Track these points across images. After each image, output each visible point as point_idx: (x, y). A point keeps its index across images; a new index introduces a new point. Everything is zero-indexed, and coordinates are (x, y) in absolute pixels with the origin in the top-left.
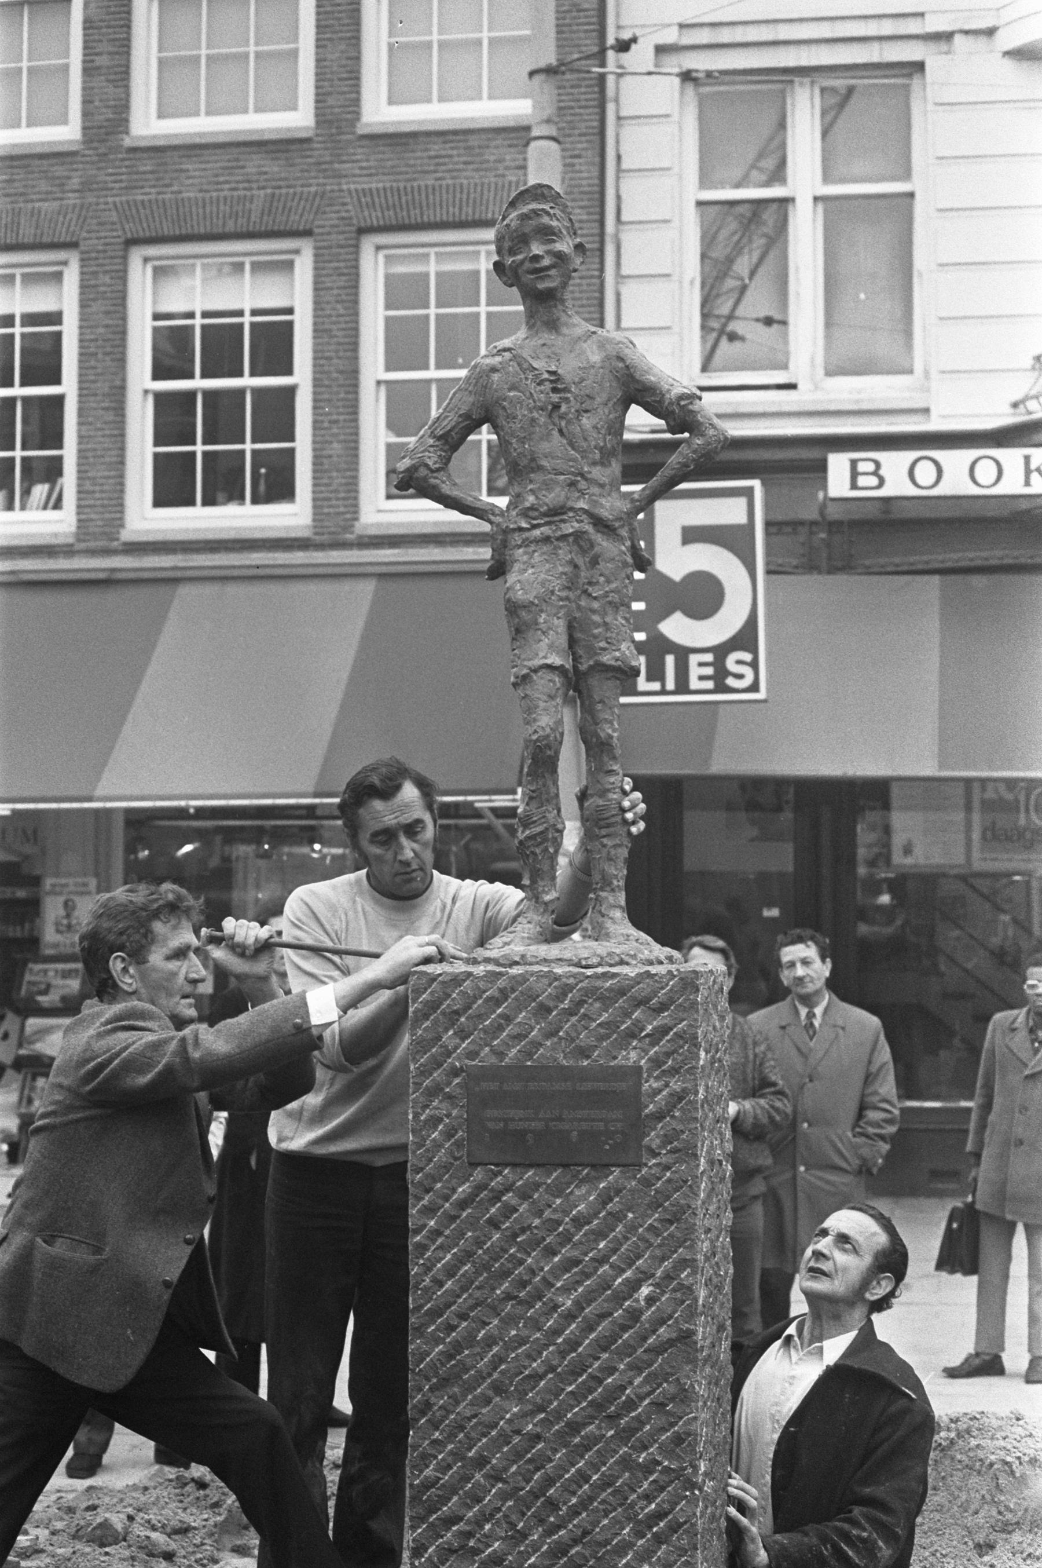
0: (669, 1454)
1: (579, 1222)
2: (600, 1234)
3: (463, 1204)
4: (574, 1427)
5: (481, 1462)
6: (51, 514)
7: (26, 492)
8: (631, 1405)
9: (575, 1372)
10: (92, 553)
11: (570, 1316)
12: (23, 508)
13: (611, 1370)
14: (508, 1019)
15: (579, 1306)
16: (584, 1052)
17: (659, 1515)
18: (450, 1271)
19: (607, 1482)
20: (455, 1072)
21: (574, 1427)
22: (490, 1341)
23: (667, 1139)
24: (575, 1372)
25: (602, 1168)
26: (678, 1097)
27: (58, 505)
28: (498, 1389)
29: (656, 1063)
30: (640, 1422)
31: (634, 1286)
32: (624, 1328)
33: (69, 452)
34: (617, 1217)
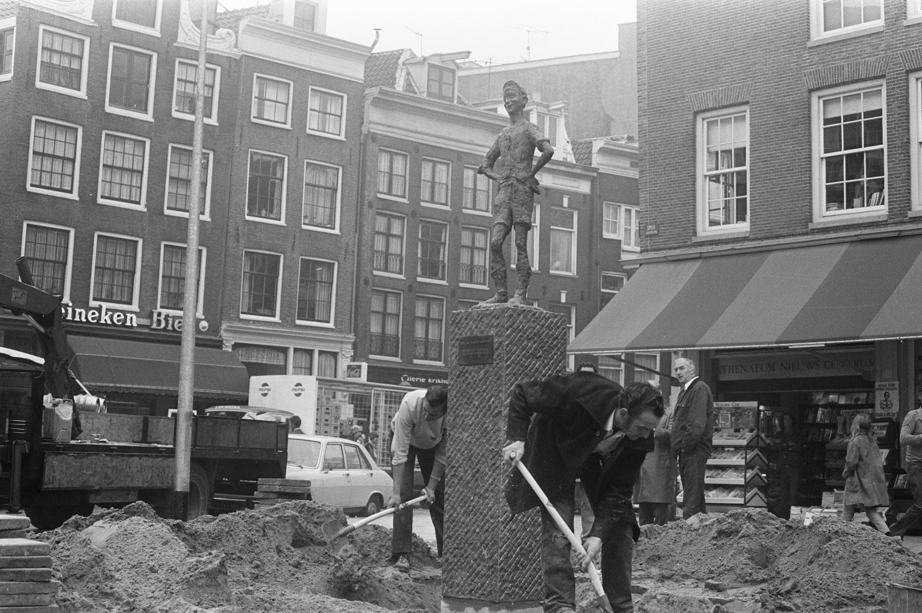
0: (496, 447)
1: (480, 380)
2: (484, 384)
3: (458, 377)
4: (478, 439)
5: (459, 450)
6: (880, 207)
7: (870, 197)
8: (488, 433)
9: (478, 424)
10: (896, 224)
11: (477, 408)
12: (868, 205)
13: (485, 423)
14: (468, 324)
15: (479, 405)
16: (482, 332)
17: (494, 464)
18: (455, 396)
19: (483, 456)
20: (457, 340)
21: (478, 439)
22: (463, 415)
23: (498, 356)
24: (478, 424)
25: (484, 364)
26: (500, 343)
27: (883, 203)
28: (464, 430)
29: (497, 334)
30: (491, 438)
31: (490, 398)
32: (488, 410)
33: (886, 177)
34: (488, 378)
